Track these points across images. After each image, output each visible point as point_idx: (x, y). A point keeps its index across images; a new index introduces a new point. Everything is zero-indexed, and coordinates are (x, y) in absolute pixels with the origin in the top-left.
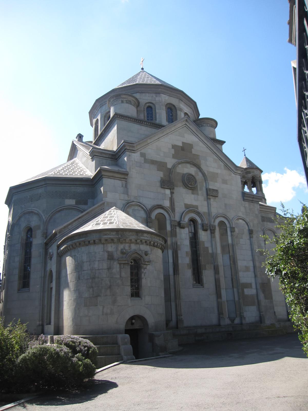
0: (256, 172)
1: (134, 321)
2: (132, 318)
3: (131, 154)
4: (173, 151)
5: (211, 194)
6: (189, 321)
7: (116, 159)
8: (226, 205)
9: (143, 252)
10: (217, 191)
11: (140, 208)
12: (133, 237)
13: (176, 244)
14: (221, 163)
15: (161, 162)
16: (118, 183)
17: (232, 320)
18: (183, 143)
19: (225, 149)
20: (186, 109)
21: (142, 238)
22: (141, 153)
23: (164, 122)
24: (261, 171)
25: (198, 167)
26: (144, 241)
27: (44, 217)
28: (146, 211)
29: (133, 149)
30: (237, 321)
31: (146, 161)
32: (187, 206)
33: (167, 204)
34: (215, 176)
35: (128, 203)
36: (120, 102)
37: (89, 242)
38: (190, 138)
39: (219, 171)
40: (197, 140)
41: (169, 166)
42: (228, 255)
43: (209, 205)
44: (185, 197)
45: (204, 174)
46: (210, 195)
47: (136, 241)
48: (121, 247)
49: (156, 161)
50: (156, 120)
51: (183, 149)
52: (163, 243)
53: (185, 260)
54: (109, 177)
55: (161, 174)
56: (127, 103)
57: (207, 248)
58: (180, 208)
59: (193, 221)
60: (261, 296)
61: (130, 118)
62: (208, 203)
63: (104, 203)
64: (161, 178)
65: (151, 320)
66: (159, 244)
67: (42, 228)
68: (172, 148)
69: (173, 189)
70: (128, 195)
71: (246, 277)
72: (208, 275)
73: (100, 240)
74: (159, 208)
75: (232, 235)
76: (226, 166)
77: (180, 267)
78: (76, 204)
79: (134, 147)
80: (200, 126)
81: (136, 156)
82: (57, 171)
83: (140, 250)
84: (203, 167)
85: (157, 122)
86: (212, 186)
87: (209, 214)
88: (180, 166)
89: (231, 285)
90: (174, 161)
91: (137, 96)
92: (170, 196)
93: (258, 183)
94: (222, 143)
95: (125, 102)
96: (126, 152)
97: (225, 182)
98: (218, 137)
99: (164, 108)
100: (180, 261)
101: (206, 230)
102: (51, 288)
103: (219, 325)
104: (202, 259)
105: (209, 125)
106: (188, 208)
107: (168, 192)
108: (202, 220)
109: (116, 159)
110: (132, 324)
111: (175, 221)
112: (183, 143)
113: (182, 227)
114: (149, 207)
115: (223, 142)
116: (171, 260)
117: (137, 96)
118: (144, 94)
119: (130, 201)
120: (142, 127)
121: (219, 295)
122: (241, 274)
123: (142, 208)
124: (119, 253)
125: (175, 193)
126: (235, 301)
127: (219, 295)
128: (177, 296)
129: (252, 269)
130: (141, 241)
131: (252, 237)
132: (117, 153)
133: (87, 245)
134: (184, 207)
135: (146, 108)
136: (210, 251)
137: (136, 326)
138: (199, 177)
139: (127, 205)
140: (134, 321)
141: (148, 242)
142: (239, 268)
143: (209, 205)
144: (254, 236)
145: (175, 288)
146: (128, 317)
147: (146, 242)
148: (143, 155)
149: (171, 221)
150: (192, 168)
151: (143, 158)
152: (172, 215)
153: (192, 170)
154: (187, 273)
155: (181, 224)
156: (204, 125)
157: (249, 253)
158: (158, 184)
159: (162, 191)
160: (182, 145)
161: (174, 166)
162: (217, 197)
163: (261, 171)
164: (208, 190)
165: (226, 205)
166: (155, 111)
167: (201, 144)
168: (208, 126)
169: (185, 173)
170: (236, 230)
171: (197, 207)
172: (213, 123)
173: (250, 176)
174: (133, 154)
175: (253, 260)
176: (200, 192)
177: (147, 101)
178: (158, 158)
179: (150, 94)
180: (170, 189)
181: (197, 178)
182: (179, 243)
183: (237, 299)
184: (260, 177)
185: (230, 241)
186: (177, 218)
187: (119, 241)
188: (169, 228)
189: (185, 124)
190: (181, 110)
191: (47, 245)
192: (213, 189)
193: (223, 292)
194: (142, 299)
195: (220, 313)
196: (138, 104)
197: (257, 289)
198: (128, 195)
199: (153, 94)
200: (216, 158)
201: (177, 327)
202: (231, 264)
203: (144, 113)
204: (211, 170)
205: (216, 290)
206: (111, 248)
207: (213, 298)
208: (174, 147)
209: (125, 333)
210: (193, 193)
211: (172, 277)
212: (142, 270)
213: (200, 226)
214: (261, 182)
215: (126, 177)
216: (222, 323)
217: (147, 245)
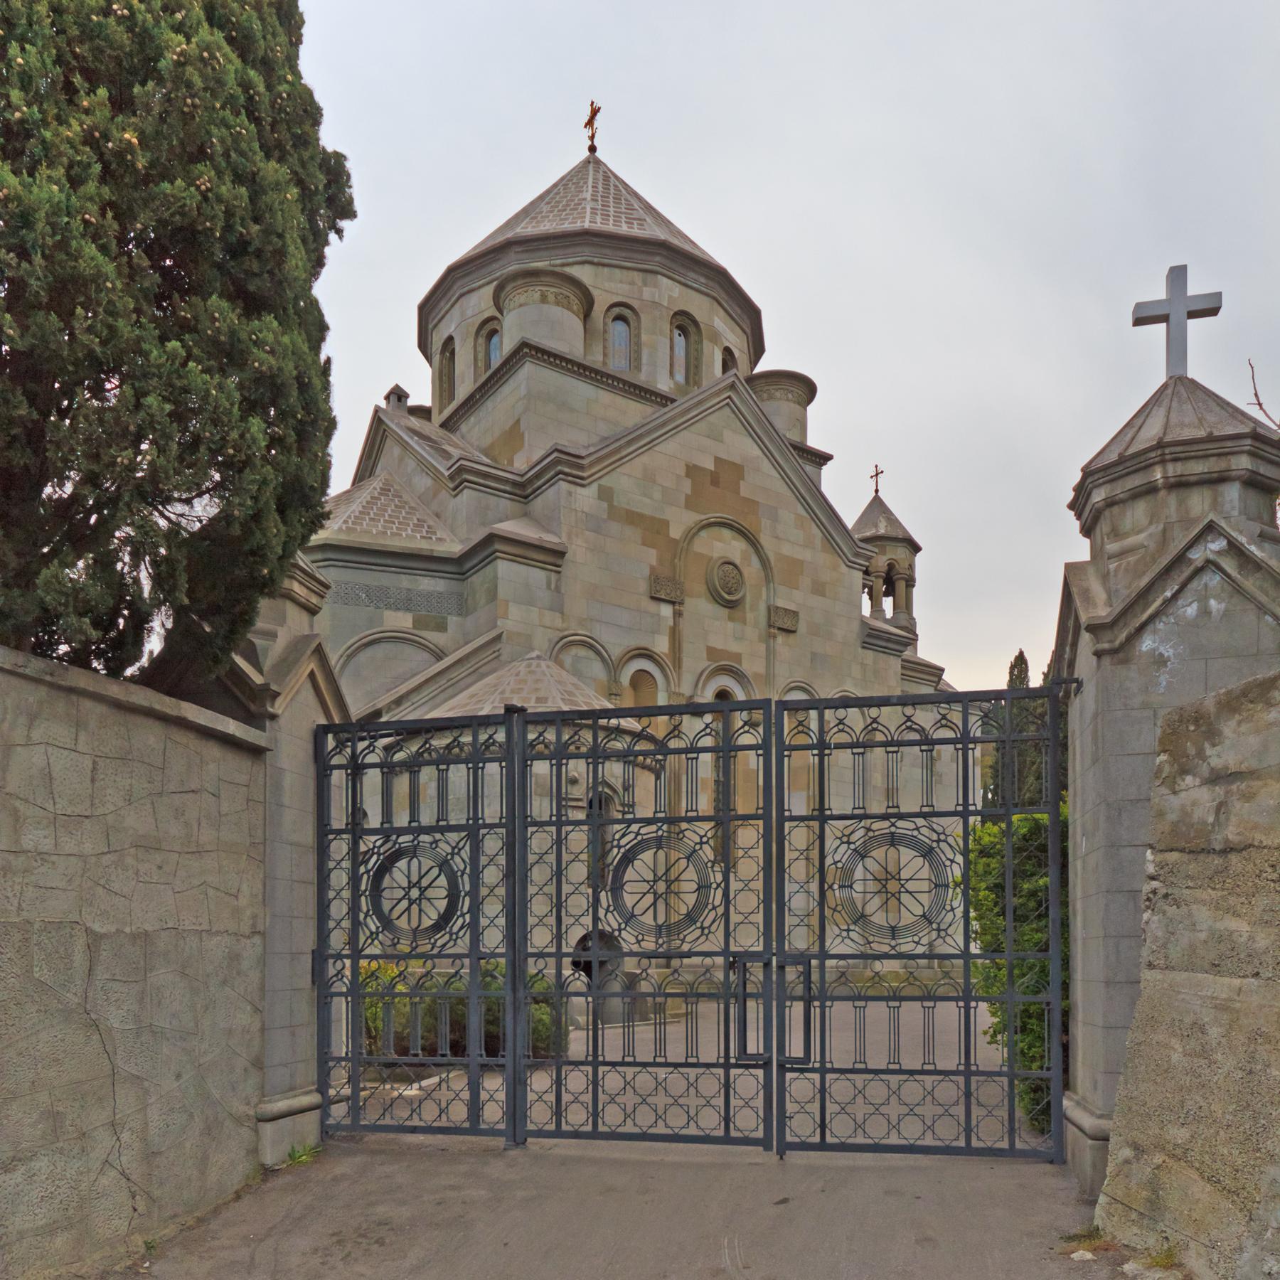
4: (687, 487)
5: (781, 624)
8: (814, 656)
10: (795, 614)
11: (591, 654)
14: (815, 530)
15: (652, 519)
16: (538, 576)
18: (718, 460)
19: (831, 481)
22: (600, 486)
23: (664, 385)
29: (581, 474)
31: (614, 513)
32: (712, 653)
33: (661, 645)
34: (795, 567)
36: (537, 296)
39: (807, 555)
40: (757, 452)
41: (676, 532)
43: (770, 655)
44: (710, 627)
45: (765, 562)
49: (641, 516)
51: (715, 480)
54: (515, 558)
55: (651, 556)
56: (557, 303)
58: (695, 662)
61: (568, 361)
62: (768, 649)
64: (652, 569)
68: (688, 475)
69: (681, 603)
70: (562, 613)
76: (828, 538)
78: (414, 627)
80: (765, 395)
82: (349, 517)
84: (765, 540)
88: (703, 534)
90: (692, 518)
91: (584, 274)
92: (671, 623)
94: (822, 459)
95: (551, 298)
96: (561, 482)
97: (819, 589)
98: (814, 441)
99: (667, 327)
105: (790, 396)
107: (666, 611)
109: (526, 497)
111: (680, 694)
112: (718, 460)
114: (616, 651)
118: (606, 270)
120: (601, 392)
132: (530, 481)
135: (609, 320)
138: (752, 570)
143: (770, 655)
148: (605, 494)
150: (735, 543)
151: (605, 505)
152: (673, 675)
153: (734, 548)
156: (778, 394)
159: (652, 607)
162: (794, 632)
164: (772, 610)
165: (814, 656)
166: (638, 336)
167: (766, 466)
168: (788, 400)
169: (715, 555)
171: (738, 657)
172: (805, 388)
174: (579, 489)
176: (750, 616)
178: (645, 506)
179: (625, 272)
180: (673, 603)
190: (715, 337)
192: (786, 610)
198: (562, 613)
199: (635, 273)
200: (804, 514)
204: (787, 550)
210: (731, 619)
215: (559, 562)
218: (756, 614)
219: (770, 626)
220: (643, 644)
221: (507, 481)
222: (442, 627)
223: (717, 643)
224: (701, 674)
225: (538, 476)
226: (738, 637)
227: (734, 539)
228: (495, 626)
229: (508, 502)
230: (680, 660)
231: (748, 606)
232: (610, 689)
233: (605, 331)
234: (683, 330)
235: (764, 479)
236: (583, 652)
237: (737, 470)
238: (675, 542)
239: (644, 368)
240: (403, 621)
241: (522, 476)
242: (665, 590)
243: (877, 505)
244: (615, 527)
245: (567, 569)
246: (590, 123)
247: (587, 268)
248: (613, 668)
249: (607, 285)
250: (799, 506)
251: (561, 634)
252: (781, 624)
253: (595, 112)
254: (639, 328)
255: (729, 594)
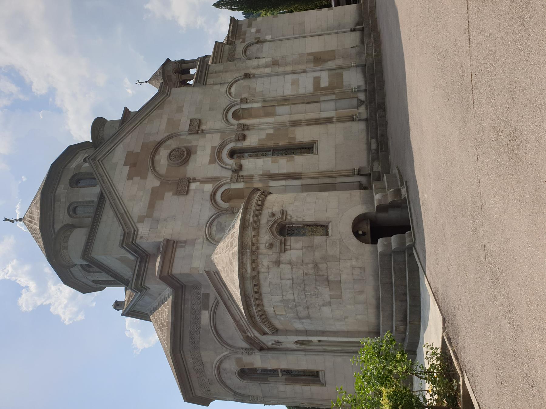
0: (170, 68)
1: (360, 232)
2: (356, 234)
3: (139, 236)
4: (137, 179)
5: (196, 127)
6: (360, 160)
7: (147, 255)
8: (210, 109)
9: (270, 219)
10: (191, 120)
12: (250, 232)
13: (261, 175)
14: (154, 114)
15: (152, 194)
16: (180, 253)
17: (361, 103)
18: (125, 164)
19: (134, 108)
20: (79, 159)
21: (251, 221)
22: (138, 222)
23: (97, 190)
24: (168, 60)
25: (159, 145)
26: (255, 219)
27: (225, 353)
28: (219, 215)
30: (362, 96)
32: (212, 162)
33: (209, 188)
35: (207, 239)
37: (256, 293)
38: (119, 155)
40: (121, 145)
41: (157, 183)
42: (277, 108)
43: (211, 131)
44: (201, 164)
45: (169, 138)
46: (197, 129)
47: (255, 229)
48: (263, 248)
50: (93, 202)
51: (133, 165)
52: (259, 193)
53: (283, 164)
55: (168, 195)
57: (267, 135)
58: (215, 171)
59: (232, 154)
60: (331, 64)
61: (89, 236)
62: (209, 133)
63: (206, 271)
64: (173, 195)
65: (359, 210)
66: (260, 199)
67: (239, 356)
68: (132, 179)
69: (189, 179)
71: (306, 84)
72: (303, 135)
73: (254, 277)
74: (214, 198)
75: (251, 102)
77: (291, 170)
78: (208, 309)
79: (129, 233)
81: (143, 230)
83: (267, 223)
84: (159, 138)
85: (96, 200)
86: (185, 126)
87: (222, 132)
88: (157, 169)
89: (316, 104)
91: (58, 227)
92: (198, 183)
93: (184, 66)
94: (126, 110)
97: (180, 110)
98: (119, 117)
100: (284, 171)
101: (244, 137)
102: (319, 341)
103: (366, 120)
104: (282, 142)
105: (101, 129)
106: (216, 160)
107: (193, 186)
108: (231, 141)
110: (364, 234)
112: (125, 164)
113: (241, 167)
114: (213, 211)
115: (126, 110)
116: (283, 183)
117: (58, 227)
119: (205, 237)
121: (328, 121)
122: (302, 91)
123: (214, 220)
124: (270, 252)
125: (195, 176)
126: (336, 100)
127: (328, 121)
128: (328, 174)
129: (295, 76)
130: (255, 222)
131: (254, 75)
133: (261, 295)
134: (213, 165)
136: (272, 131)
137: (366, 228)
138: (173, 144)
139: (210, 240)
140: (360, 232)
141: (257, 213)
142: (294, 93)
143: (211, 131)
144: (253, 71)
145: (318, 178)
146: (355, 240)
147: (257, 216)
148: (141, 220)
149: (232, 182)
150: (161, 154)
152: (223, 181)
154: (300, 163)
155: (236, 169)
156: (101, 135)
157: (274, 79)
158: (182, 199)
159: (191, 193)
160: (129, 167)
161: (158, 175)
163: (168, 60)
165: (210, 109)
166: (80, 202)
167: (127, 140)
168: (103, 130)
169: (167, 163)
170: (244, 96)
171: (213, 148)
173: (174, 77)
174: (140, 233)
175: (284, 74)
176: (194, 143)
177: (66, 214)
178: (145, 199)
180: (189, 182)
181: (174, 146)
182: (261, 173)
183: (334, 97)
184: (175, 62)
185: (259, 105)
186: (229, 174)
187: (255, 252)
188: (241, 185)
189: (98, 161)
190: (79, 167)
191: (262, 349)
193: (325, 115)
194: (331, 221)
195: (351, 119)
196: (71, 227)
197: (321, 70)
200: (147, 120)
201: (368, 175)
202: (288, 104)
203: (83, 217)
204: (163, 127)
205: (321, 124)
206: (265, 262)
207: (331, 126)
208: (130, 177)
209: (377, 243)
210: (195, 153)
211: (305, 182)
212: (293, 220)
213: (239, 145)
214: (183, 62)
215: (172, 242)
216: (364, 116)
217: (260, 214)
218: (194, 140)
219: (198, 133)
220: (208, 197)
221: (140, 265)
222: (207, 296)
223: (207, 159)
224: (222, 167)
225: (136, 252)
226: (204, 148)
227: (159, 154)
228: (202, 274)
229: (150, 264)
230: (215, 178)
231: (190, 145)
232: (230, 213)
233: (80, 217)
234: (78, 182)
235: (132, 142)
236: (214, 228)
237: (130, 154)
238: (162, 183)
239: (93, 199)
240: (205, 316)
241: (137, 258)
242: (182, 187)
243: (150, 81)
244: (156, 214)
245: (176, 238)
246: (12, 221)
247: (55, 227)
248: (220, 212)
249: (62, 217)
250: (144, 122)
251: (205, 239)
252: (196, 127)
253: (7, 220)
254: (77, 202)
255: (184, 155)
